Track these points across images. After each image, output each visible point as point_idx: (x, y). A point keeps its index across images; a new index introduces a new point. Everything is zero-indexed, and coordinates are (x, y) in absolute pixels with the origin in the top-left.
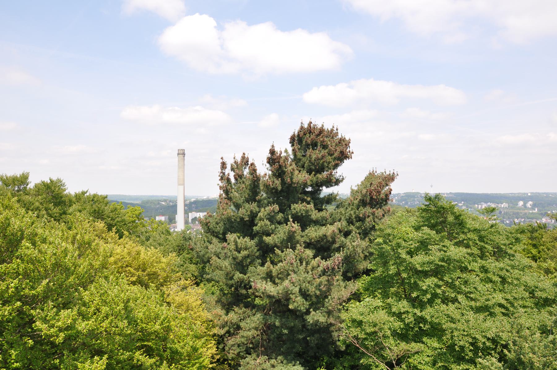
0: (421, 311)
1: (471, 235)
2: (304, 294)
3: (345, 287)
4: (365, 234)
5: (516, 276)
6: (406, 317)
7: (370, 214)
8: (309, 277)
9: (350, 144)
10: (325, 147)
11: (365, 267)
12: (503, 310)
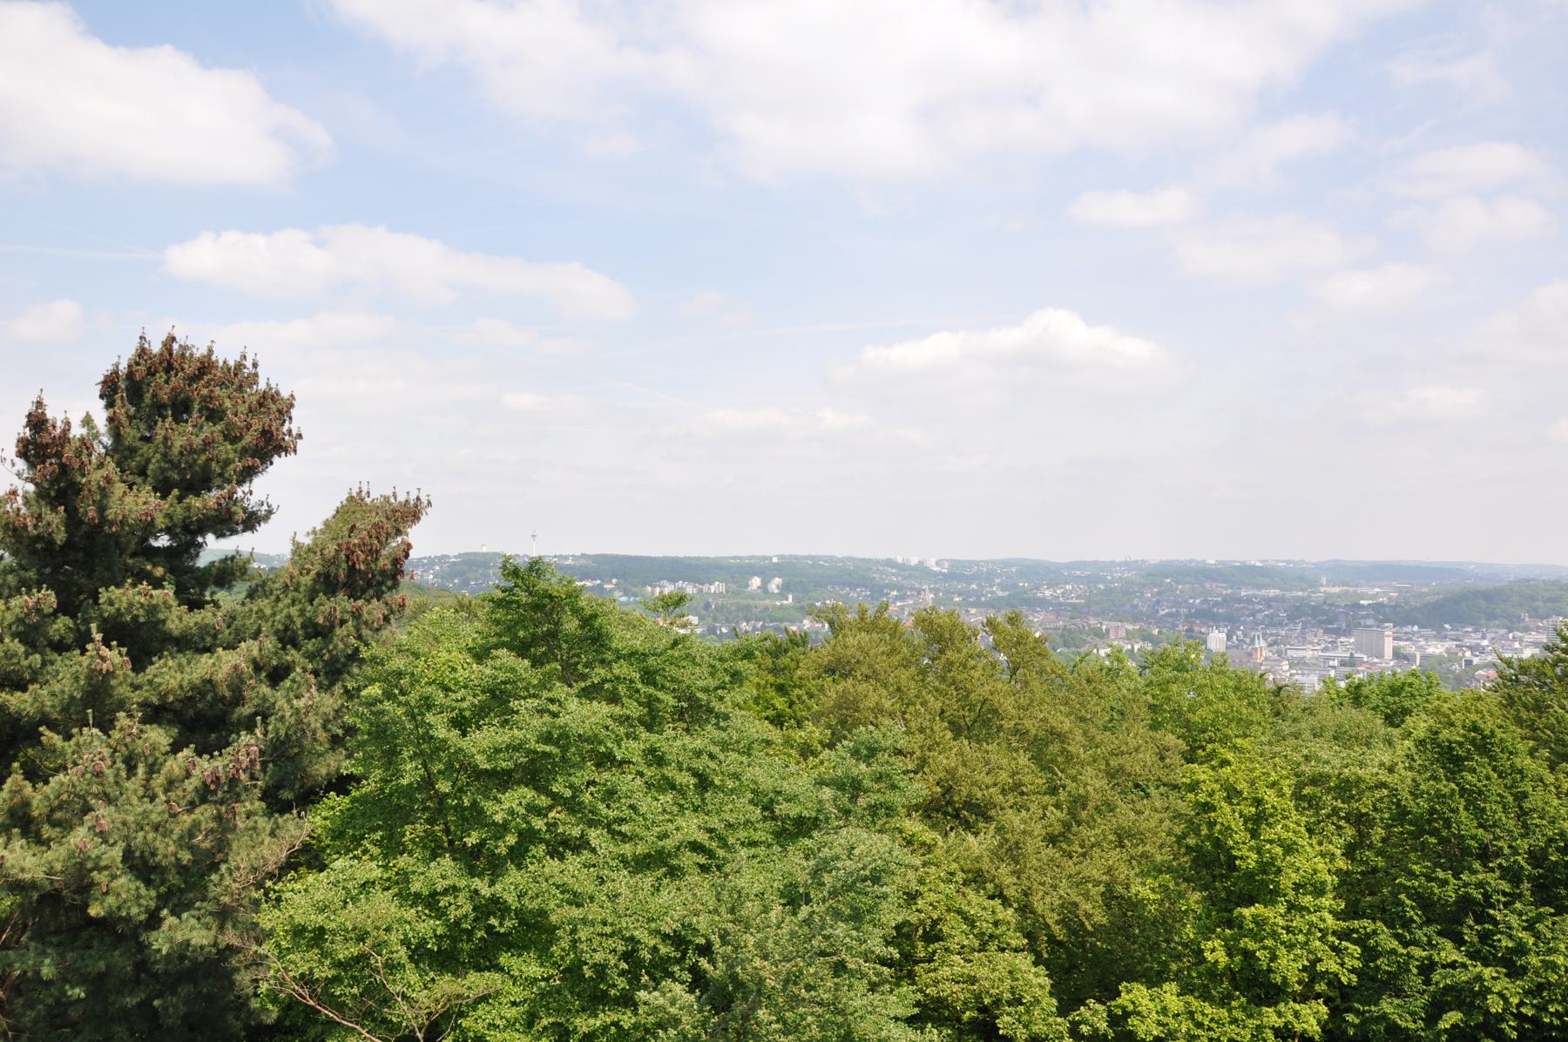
0: (492, 883)
1: (621, 669)
2: (141, 865)
3: (272, 834)
4: (332, 672)
5: (732, 769)
6: (450, 904)
7: (347, 616)
8: (157, 811)
9: (293, 412)
10: (214, 415)
11: (333, 769)
12: (702, 860)
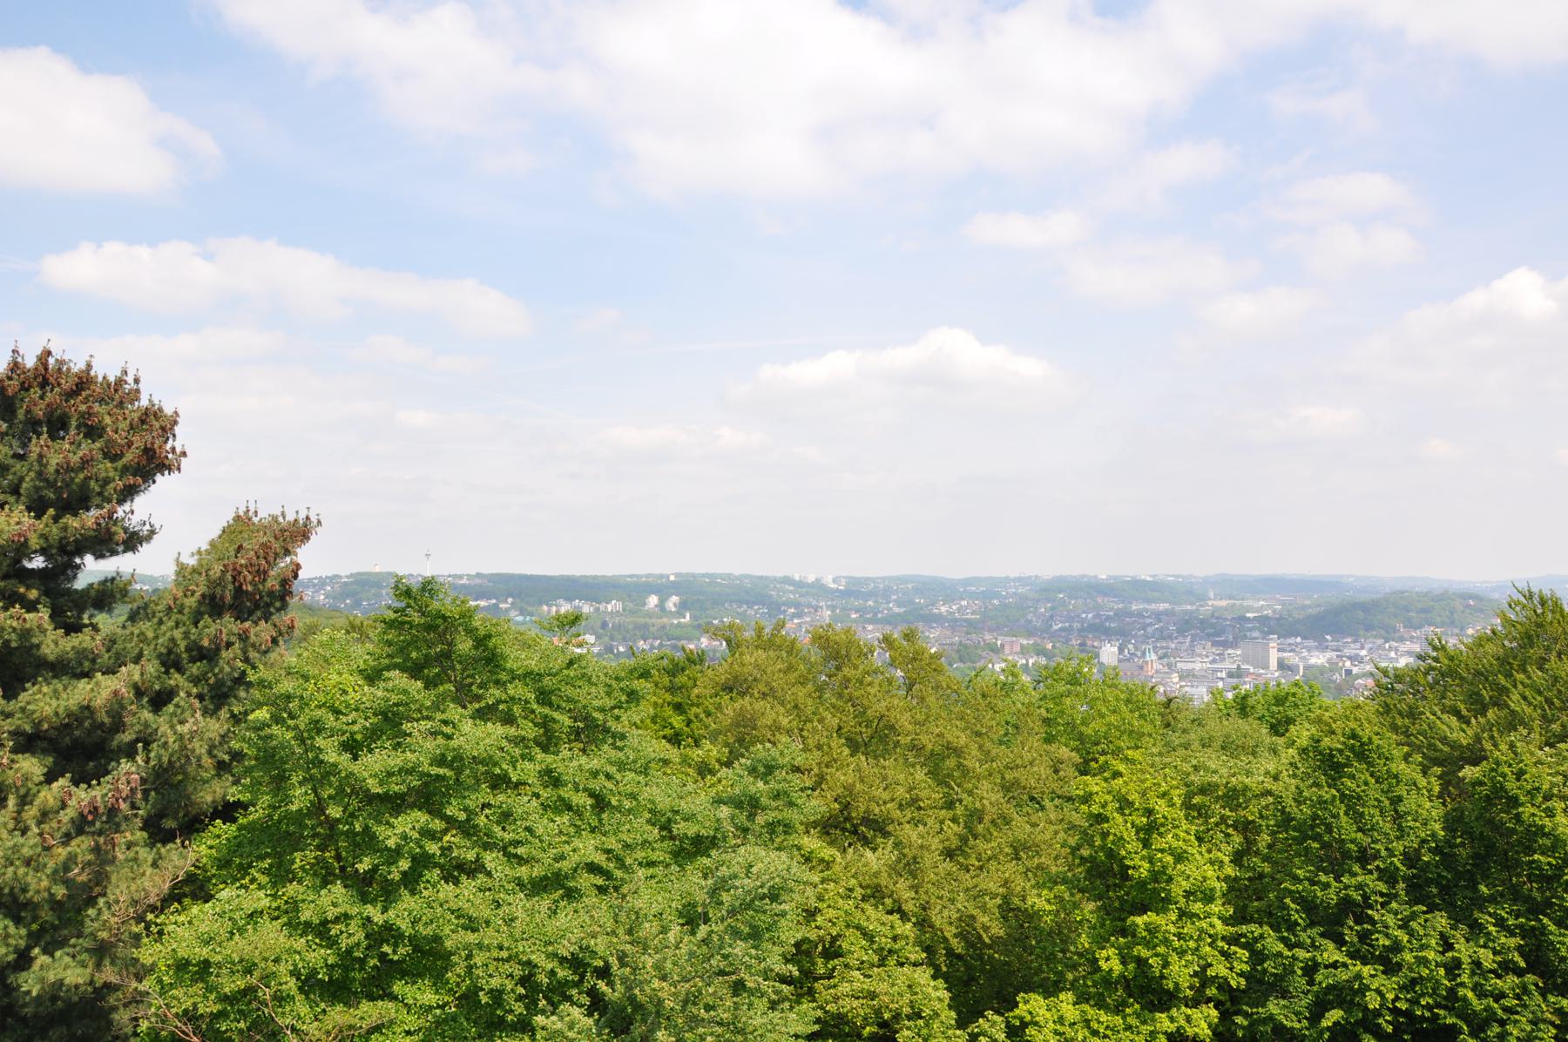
0: (385, 910)
1: (516, 690)
3: (155, 865)
4: (218, 696)
5: (629, 789)
6: (342, 932)
7: (233, 639)
9: (177, 429)
11: (218, 796)
12: (600, 881)
